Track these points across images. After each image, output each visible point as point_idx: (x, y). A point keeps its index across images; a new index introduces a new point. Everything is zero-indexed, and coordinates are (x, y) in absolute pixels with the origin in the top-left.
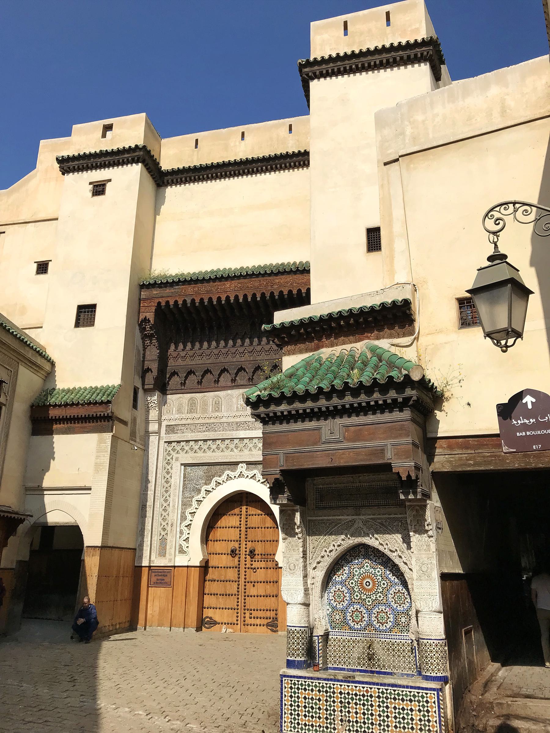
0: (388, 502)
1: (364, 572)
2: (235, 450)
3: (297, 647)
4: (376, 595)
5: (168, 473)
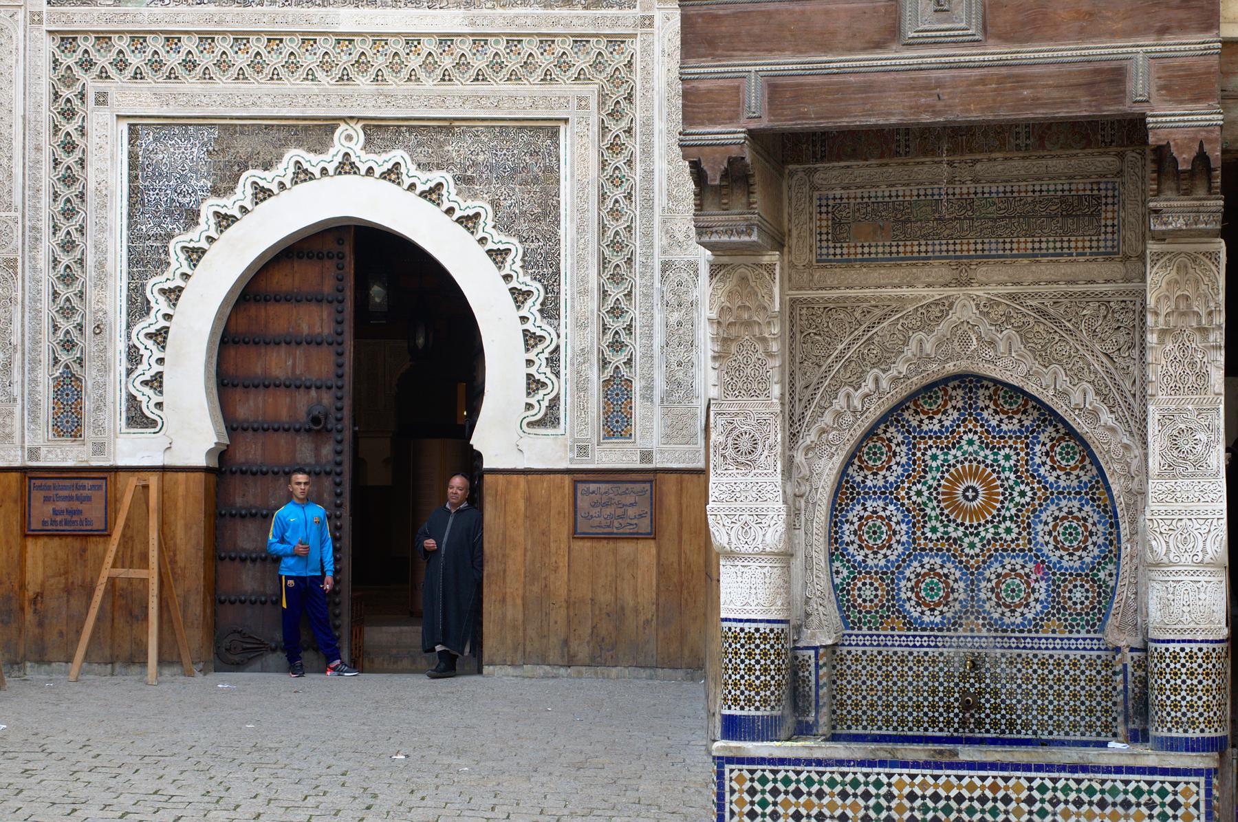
0: (1066, 245)
1: (961, 458)
2: (320, 74)
3: (763, 678)
4: (996, 527)
5: (69, 147)
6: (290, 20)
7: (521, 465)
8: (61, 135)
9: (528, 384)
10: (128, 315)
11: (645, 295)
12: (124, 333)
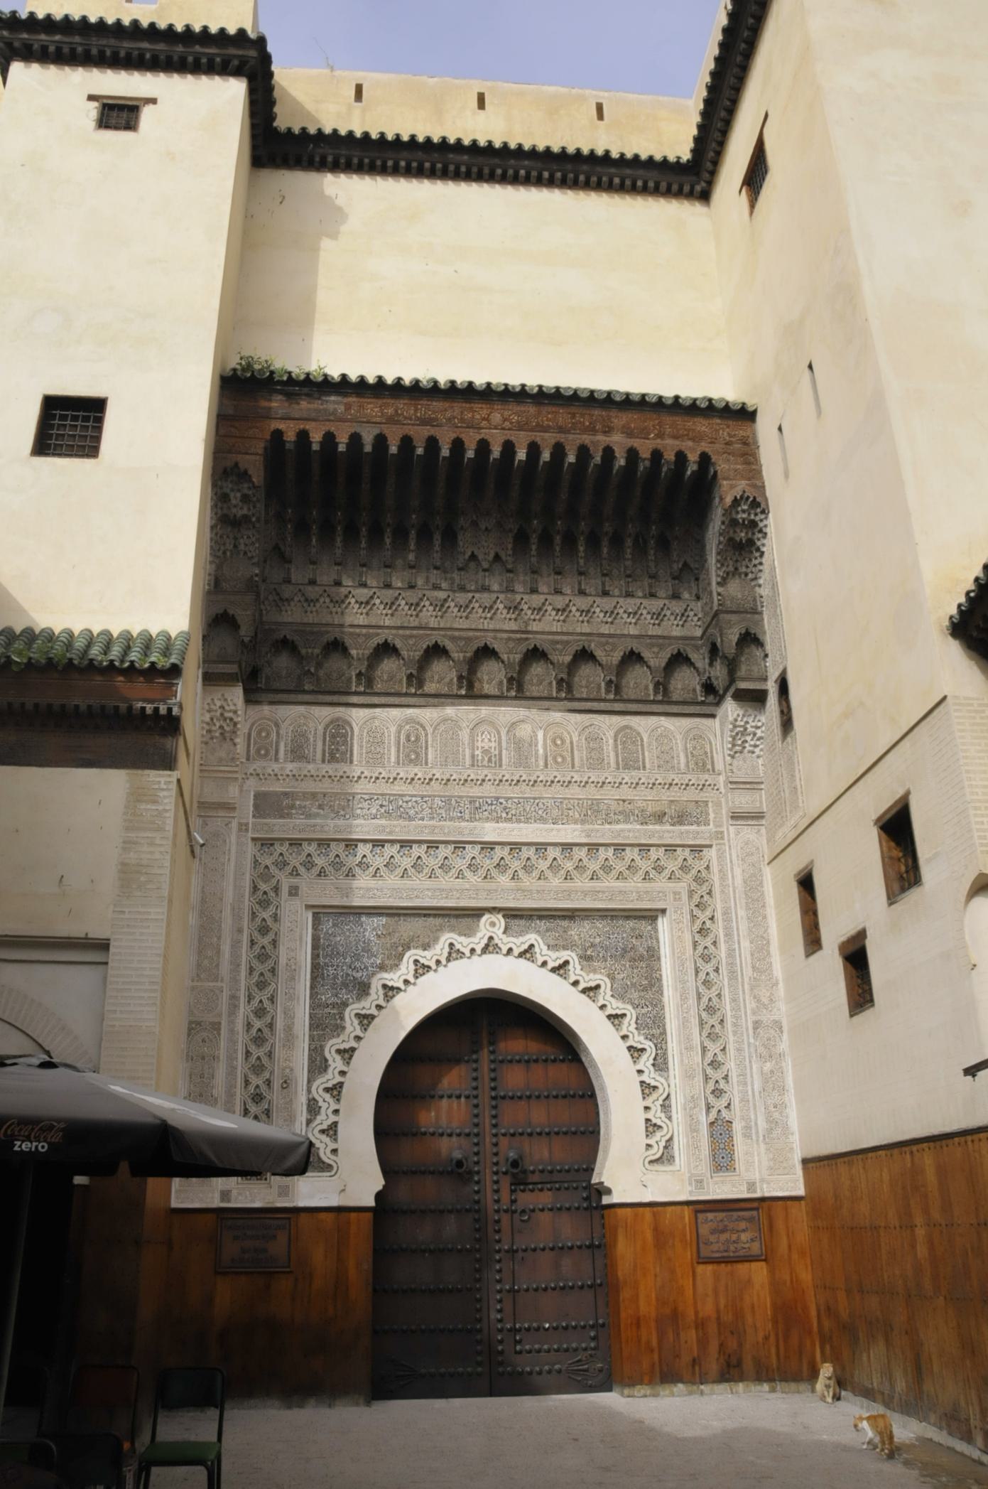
2: (468, 873)
5: (264, 930)
6: (446, 831)
7: (647, 1198)
8: (258, 920)
9: (647, 1127)
10: (309, 1072)
11: (738, 1050)
12: (305, 1087)
